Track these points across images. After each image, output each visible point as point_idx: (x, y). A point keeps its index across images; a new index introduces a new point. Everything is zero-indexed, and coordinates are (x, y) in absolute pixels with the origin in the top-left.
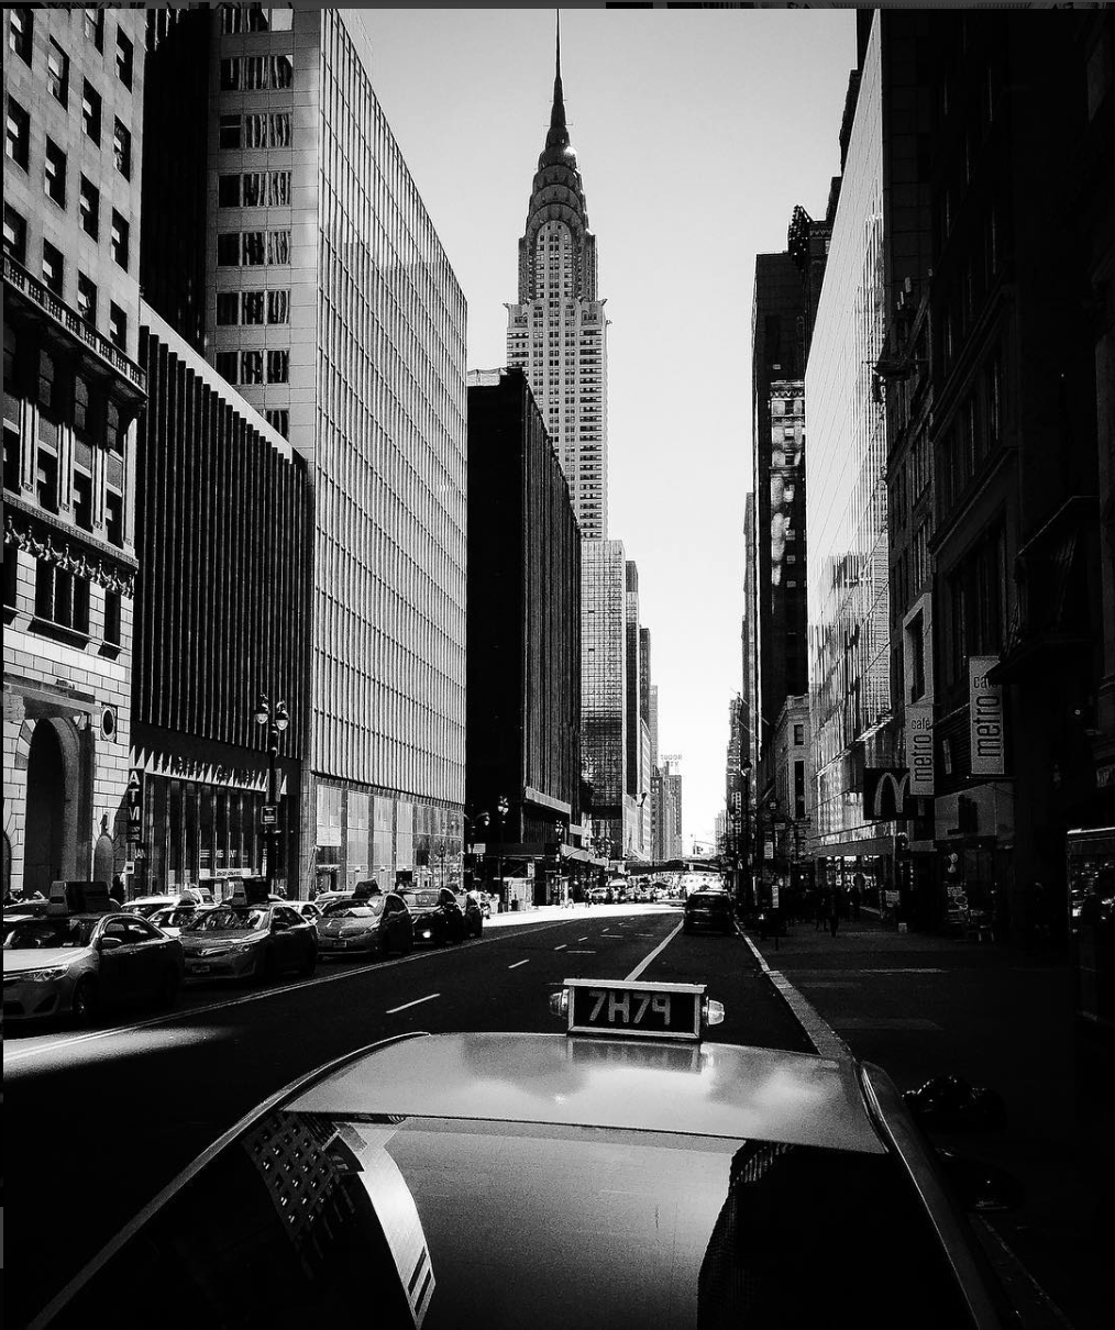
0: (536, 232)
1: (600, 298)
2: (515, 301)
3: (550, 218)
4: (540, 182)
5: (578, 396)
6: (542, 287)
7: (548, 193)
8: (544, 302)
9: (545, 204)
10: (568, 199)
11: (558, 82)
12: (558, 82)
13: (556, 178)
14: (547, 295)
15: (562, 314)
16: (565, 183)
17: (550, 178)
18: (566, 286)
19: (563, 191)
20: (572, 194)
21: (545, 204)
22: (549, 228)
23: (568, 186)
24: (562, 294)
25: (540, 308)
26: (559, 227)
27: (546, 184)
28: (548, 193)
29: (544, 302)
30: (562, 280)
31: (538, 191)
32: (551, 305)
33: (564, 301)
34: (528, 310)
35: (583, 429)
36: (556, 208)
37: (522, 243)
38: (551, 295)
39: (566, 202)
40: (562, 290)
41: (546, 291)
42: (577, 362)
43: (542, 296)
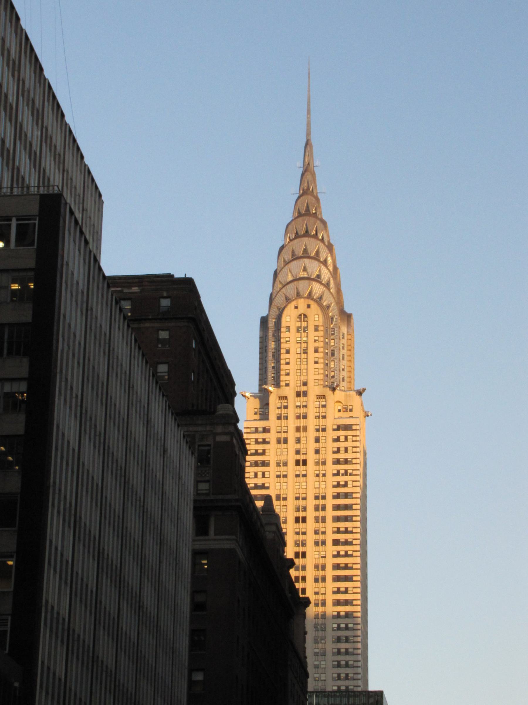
0: (281, 311)
3: (298, 295)
4: (287, 256)
5: (330, 537)
8: (289, 392)
10: (319, 276)
13: (305, 250)
16: (316, 257)
22: (296, 307)
23: (319, 260)
24: (310, 383)
25: (286, 398)
26: (309, 306)
29: (289, 392)
32: (298, 394)
35: (336, 542)
37: (264, 321)
42: (329, 519)
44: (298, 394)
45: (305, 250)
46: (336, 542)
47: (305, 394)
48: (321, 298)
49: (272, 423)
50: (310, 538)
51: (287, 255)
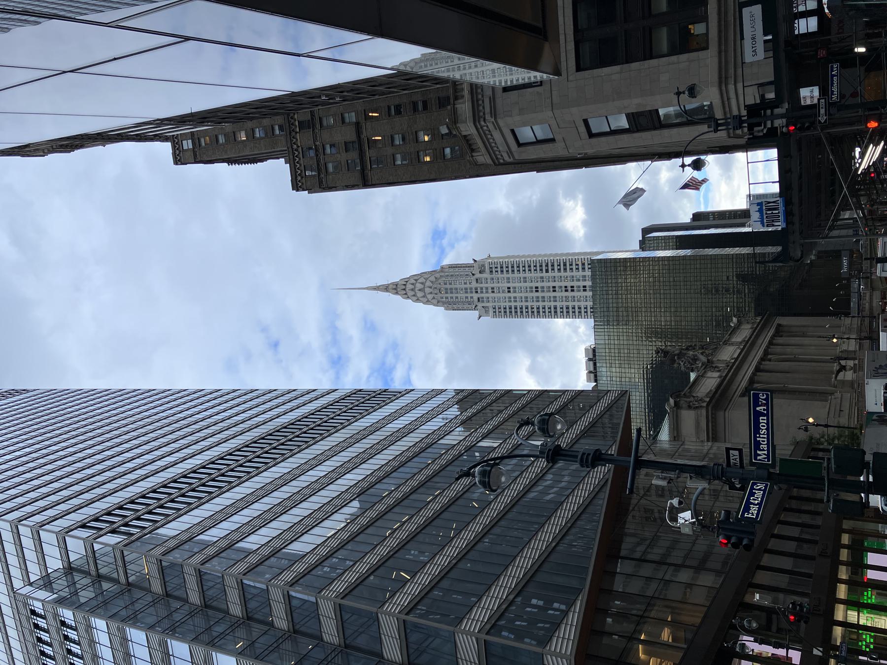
6: (467, 297)
11: (367, 288)
12: (367, 288)
13: (412, 290)
15: (481, 285)
17: (413, 293)
18: (465, 283)
19: (419, 286)
20: (420, 281)
28: (420, 294)
29: (476, 296)
30: (464, 286)
32: (477, 292)
33: (474, 285)
34: (480, 305)
35: (547, 271)
36: (427, 290)
38: (471, 292)
40: (468, 286)
41: (469, 295)
43: (472, 297)
44: (477, 292)
45: (412, 290)
47: (476, 289)
48: (432, 282)
49: (490, 305)
51: (415, 298)
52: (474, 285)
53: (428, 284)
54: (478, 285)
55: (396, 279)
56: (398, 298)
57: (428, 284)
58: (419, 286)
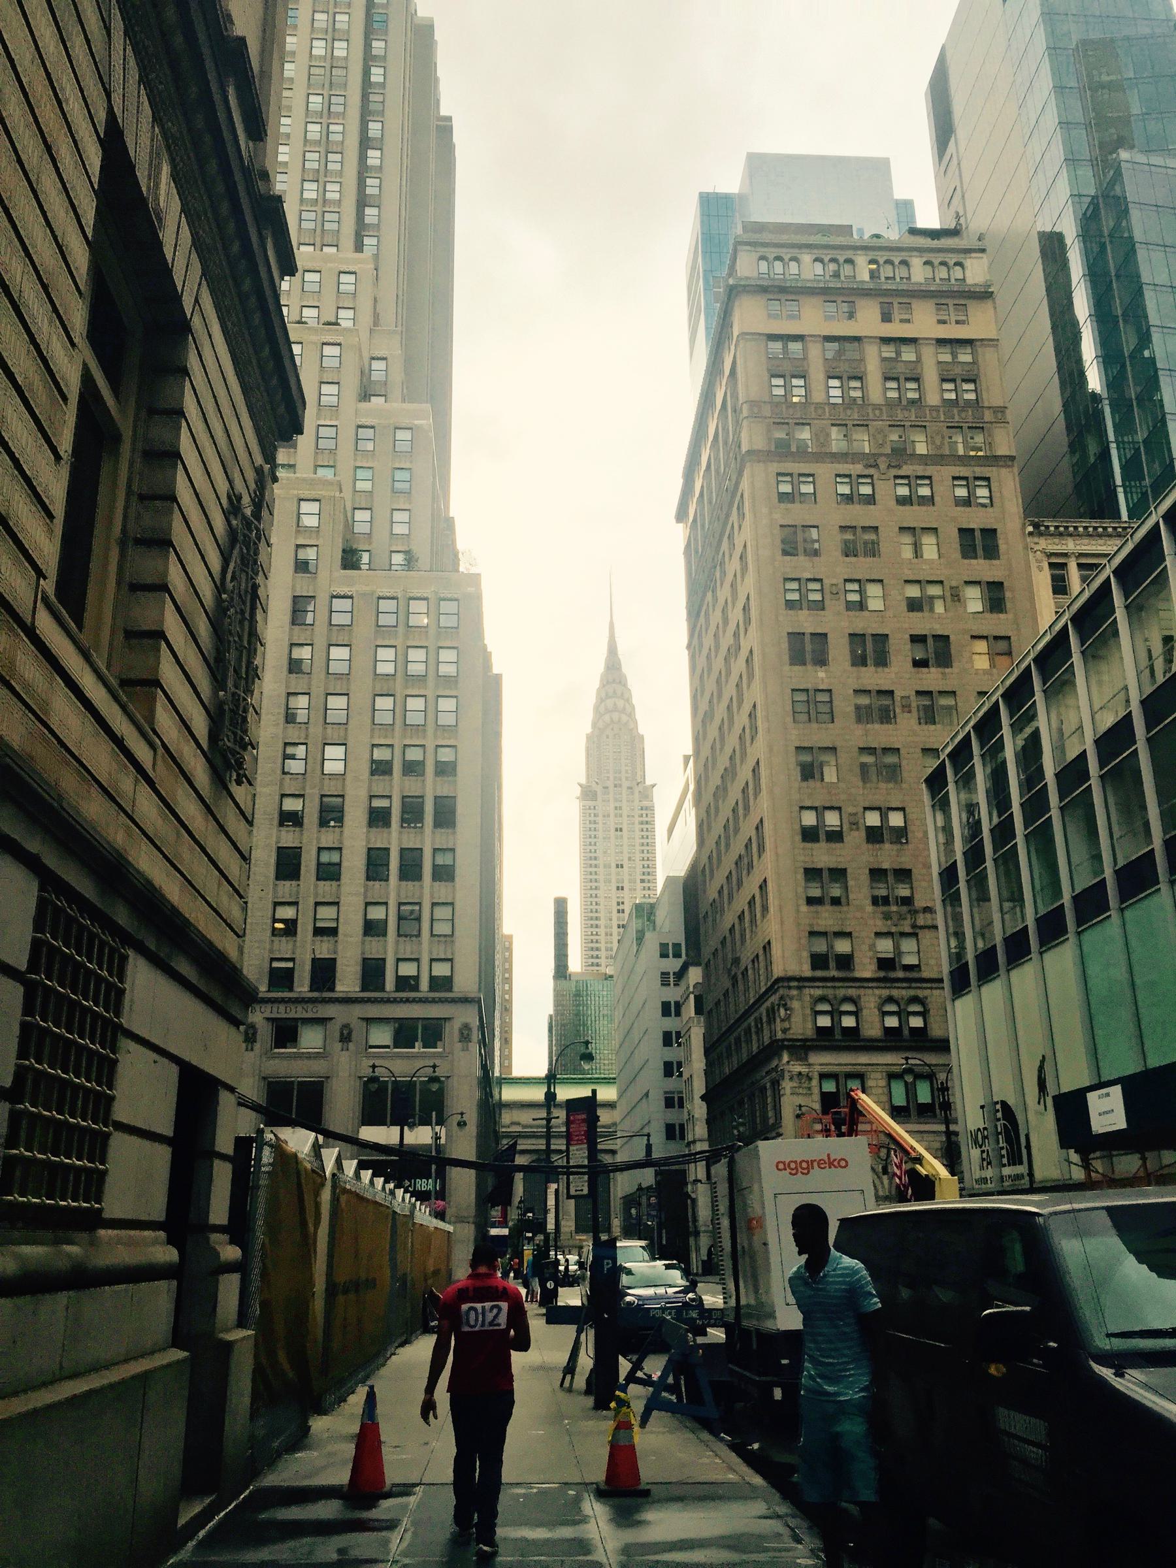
1: (648, 782)
2: (584, 781)
7: (610, 703)
9: (607, 711)
14: (612, 778)
18: (627, 772)
19: (620, 703)
21: (607, 711)
27: (608, 697)
28: (610, 703)
29: (610, 784)
31: (602, 700)
33: (626, 784)
34: (599, 789)
36: (615, 716)
38: (615, 778)
39: (623, 711)
46: (642, 881)
47: (620, 786)
50: (626, 878)
51: (603, 695)
52: (626, 784)
53: (624, 718)
54: (624, 791)
55: (625, 669)
56: (601, 668)
57: (624, 718)
58: (620, 703)
